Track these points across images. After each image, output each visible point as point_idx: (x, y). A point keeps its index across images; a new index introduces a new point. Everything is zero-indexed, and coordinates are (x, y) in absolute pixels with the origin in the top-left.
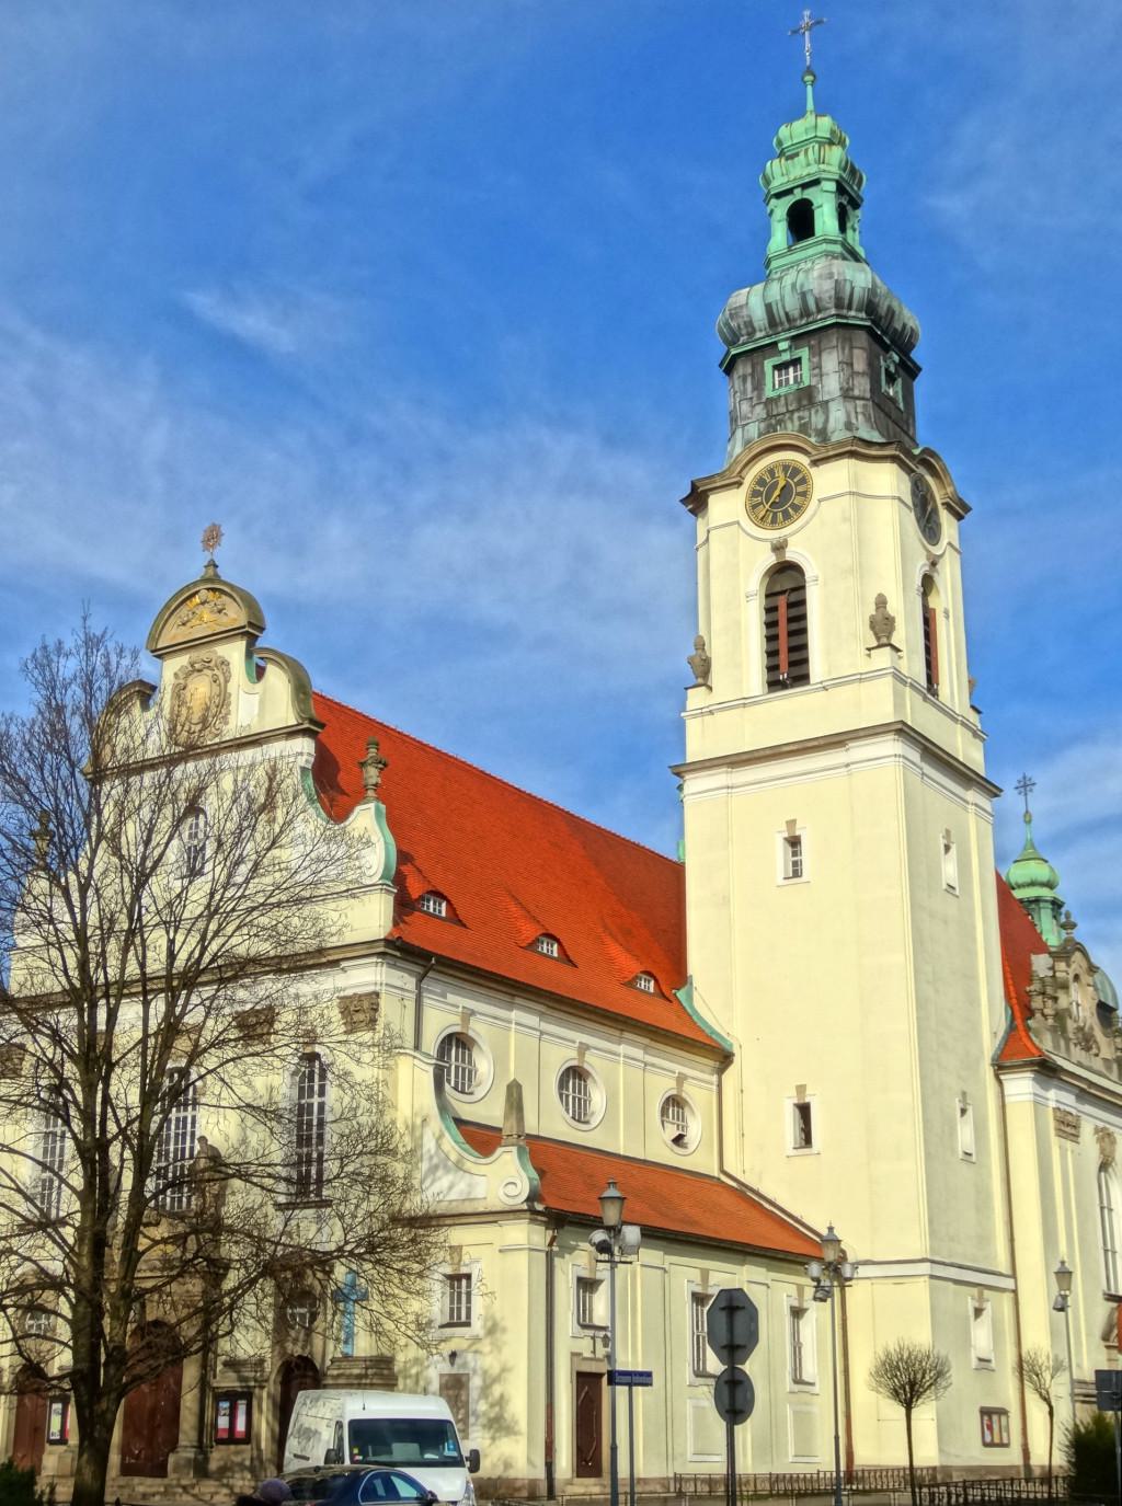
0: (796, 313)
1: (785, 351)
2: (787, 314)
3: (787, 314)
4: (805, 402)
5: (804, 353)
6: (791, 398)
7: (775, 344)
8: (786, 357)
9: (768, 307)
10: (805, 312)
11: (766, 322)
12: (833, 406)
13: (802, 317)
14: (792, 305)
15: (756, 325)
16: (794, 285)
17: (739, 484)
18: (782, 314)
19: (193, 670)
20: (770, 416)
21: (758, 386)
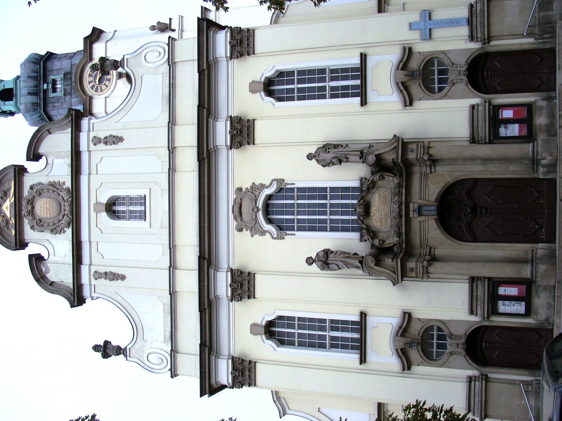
0: (35, 82)
1: (48, 86)
2: (34, 86)
3: (34, 86)
4: (69, 76)
5: (51, 77)
6: (66, 83)
7: (45, 91)
8: (50, 86)
9: (30, 94)
10: (36, 78)
11: (35, 97)
12: (73, 63)
13: (37, 80)
14: (32, 83)
15: (35, 101)
16: (24, 81)
17: (91, 98)
18: (34, 88)
19: (32, 213)
20: (71, 94)
21: (58, 99)
